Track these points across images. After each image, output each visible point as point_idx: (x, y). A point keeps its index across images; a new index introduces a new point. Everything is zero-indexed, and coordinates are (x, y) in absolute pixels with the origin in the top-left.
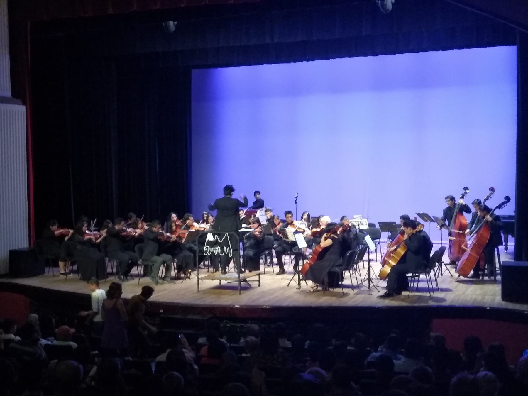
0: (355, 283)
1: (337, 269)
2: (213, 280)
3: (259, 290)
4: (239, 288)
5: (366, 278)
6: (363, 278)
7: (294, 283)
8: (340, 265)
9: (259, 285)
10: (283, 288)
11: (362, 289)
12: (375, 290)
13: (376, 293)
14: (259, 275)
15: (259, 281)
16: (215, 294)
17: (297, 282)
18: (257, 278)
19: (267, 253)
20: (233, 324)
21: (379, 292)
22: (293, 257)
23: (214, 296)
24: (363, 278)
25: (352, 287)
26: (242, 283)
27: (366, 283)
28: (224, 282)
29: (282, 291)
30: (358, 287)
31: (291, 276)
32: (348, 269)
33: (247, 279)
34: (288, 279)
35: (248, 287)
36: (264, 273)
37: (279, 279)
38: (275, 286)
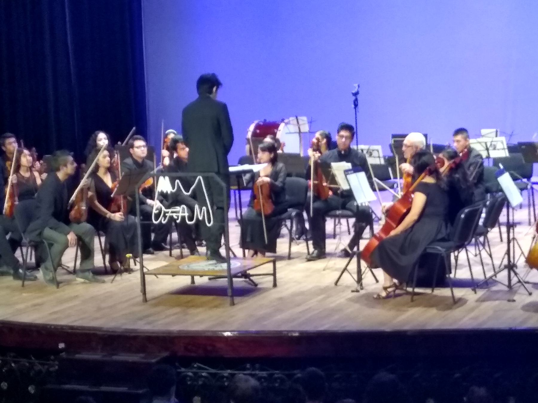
0: (478, 274)
1: (440, 248)
2: (173, 275)
3: (274, 294)
4: (229, 292)
5: (502, 267)
6: (497, 263)
7: (349, 279)
8: (443, 240)
9: (275, 285)
10: (324, 290)
11: (494, 288)
12: (522, 290)
13: (524, 297)
14: (274, 262)
15: (274, 274)
16: (179, 305)
17: (355, 276)
18: (268, 268)
19: (294, 214)
20: (213, 371)
21: (530, 294)
22: (352, 221)
23: (177, 310)
24: (497, 263)
25: (472, 284)
26: (235, 280)
27: (503, 276)
28: (200, 281)
29: (320, 297)
30: (487, 283)
31: (343, 262)
32: (461, 245)
33: (251, 272)
34: (336, 270)
35: (251, 290)
36: (289, 257)
37: (318, 271)
38: (309, 285)
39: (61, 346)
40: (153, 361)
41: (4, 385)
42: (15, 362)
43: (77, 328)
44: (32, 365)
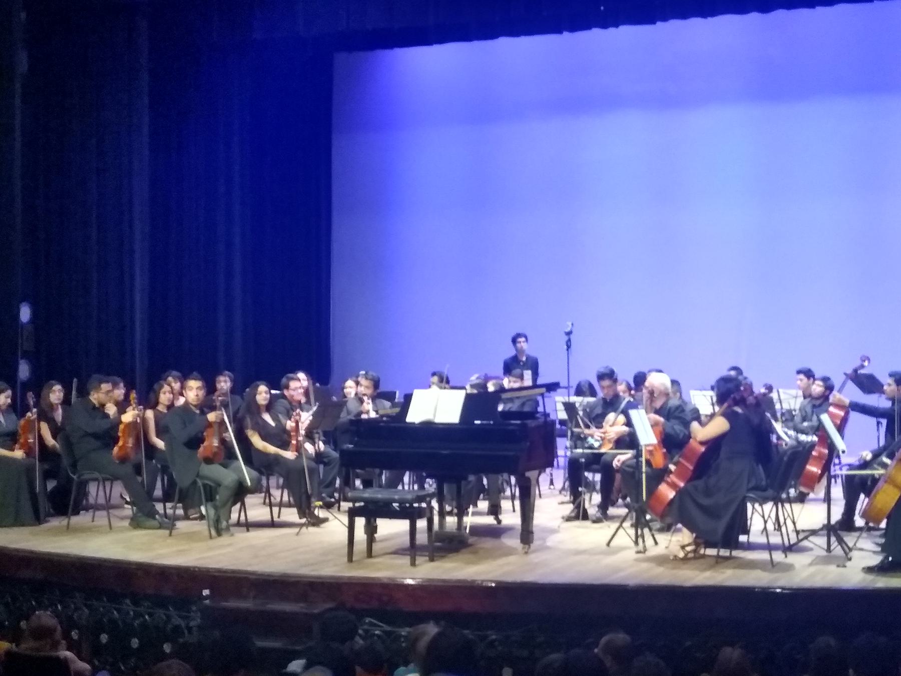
39: (206, 592)
40: (316, 611)
41: (135, 643)
42: (150, 615)
43: (226, 571)
44: (169, 617)
